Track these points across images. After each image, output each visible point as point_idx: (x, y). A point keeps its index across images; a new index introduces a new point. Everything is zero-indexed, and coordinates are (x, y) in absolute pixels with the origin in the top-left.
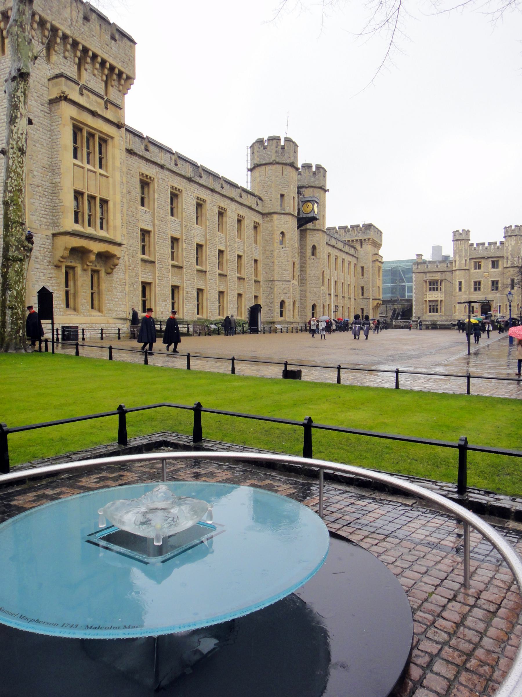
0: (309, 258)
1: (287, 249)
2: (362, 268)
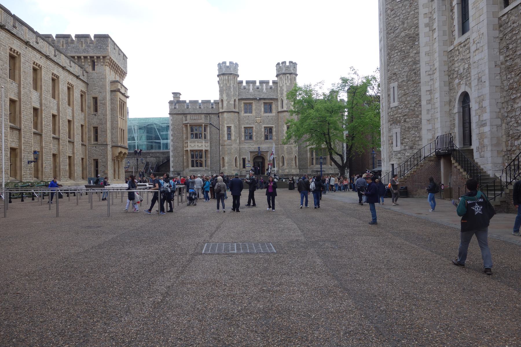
2: (95, 99)
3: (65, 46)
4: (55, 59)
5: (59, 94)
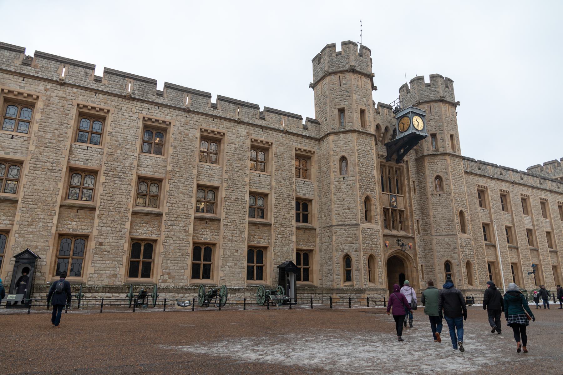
0: (432, 195)
1: (351, 178)
3: (553, 170)
4: (541, 186)
5: (550, 213)
